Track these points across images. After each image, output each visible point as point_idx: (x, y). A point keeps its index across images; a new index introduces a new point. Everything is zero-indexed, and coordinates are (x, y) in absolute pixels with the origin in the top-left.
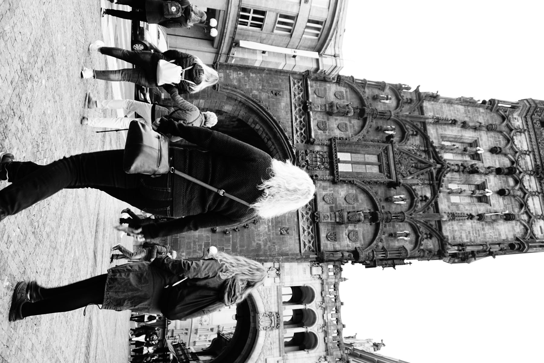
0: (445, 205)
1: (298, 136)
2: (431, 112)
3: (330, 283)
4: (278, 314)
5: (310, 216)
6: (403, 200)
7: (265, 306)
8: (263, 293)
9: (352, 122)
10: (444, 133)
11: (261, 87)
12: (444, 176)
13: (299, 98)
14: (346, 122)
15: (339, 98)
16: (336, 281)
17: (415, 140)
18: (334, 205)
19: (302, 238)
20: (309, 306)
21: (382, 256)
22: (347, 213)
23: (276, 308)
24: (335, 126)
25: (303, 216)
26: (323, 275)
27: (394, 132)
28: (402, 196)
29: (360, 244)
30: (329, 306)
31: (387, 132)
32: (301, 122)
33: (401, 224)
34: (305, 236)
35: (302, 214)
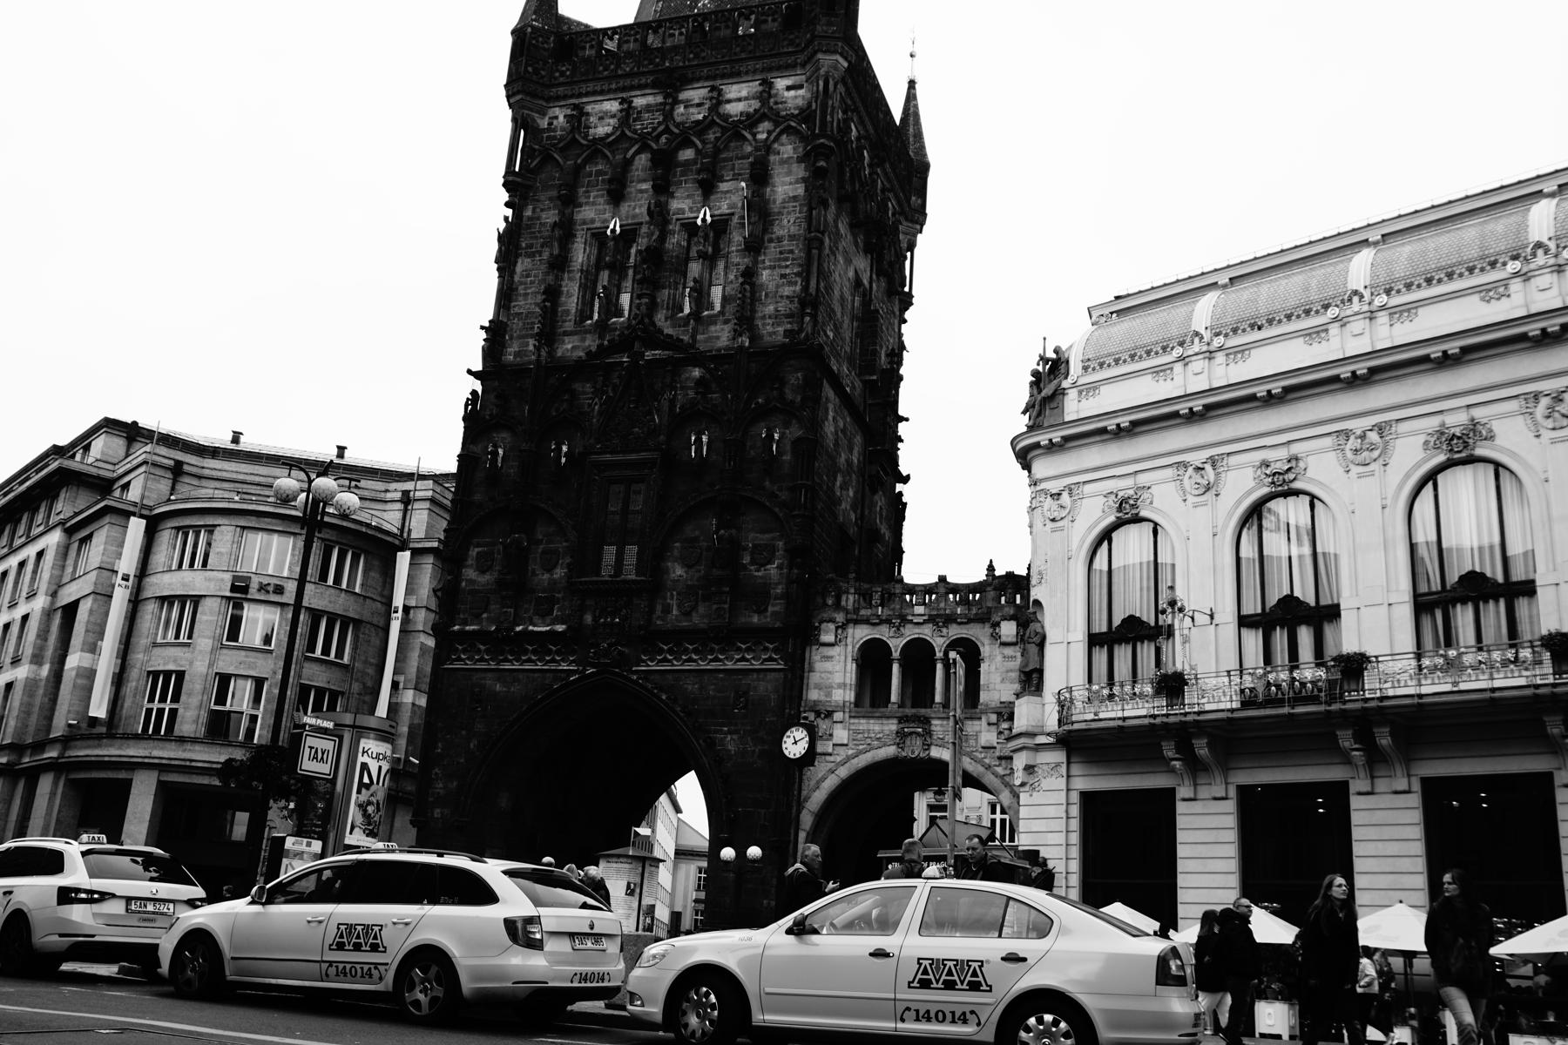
0: (723, 330)
1: (563, 660)
2: (528, 345)
3: (856, 605)
4: (901, 720)
5: (717, 644)
6: (698, 440)
7: (885, 745)
8: (861, 747)
9: (540, 537)
10: (572, 317)
11: (464, 732)
12: (660, 331)
13: (487, 652)
14: (540, 551)
15: (489, 563)
16: (852, 591)
17: (584, 393)
18: (700, 592)
19: (757, 665)
20: (896, 651)
21: (806, 495)
22: (714, 570)
23: (891, 721)
24: (546, 576)
25: (716, 660)
26: (838, 620)
27: (564, 444)
28: (693, 438)
29: (780, 540)
30: (901, 608)
31: (563, 460)
32: (534, 652)
33: (748, 444)
34: (753, 658)
35: (712, 661)
